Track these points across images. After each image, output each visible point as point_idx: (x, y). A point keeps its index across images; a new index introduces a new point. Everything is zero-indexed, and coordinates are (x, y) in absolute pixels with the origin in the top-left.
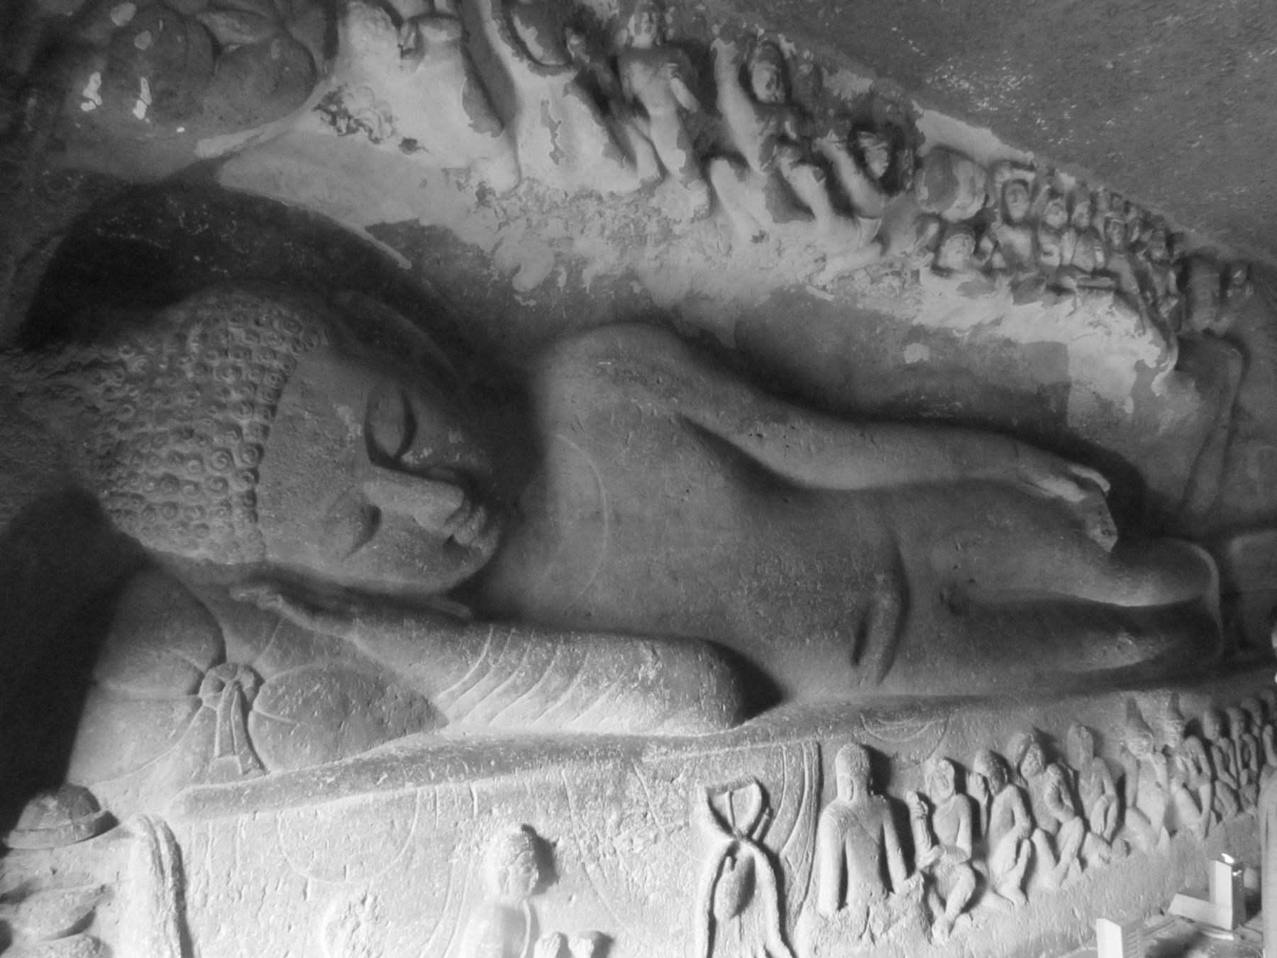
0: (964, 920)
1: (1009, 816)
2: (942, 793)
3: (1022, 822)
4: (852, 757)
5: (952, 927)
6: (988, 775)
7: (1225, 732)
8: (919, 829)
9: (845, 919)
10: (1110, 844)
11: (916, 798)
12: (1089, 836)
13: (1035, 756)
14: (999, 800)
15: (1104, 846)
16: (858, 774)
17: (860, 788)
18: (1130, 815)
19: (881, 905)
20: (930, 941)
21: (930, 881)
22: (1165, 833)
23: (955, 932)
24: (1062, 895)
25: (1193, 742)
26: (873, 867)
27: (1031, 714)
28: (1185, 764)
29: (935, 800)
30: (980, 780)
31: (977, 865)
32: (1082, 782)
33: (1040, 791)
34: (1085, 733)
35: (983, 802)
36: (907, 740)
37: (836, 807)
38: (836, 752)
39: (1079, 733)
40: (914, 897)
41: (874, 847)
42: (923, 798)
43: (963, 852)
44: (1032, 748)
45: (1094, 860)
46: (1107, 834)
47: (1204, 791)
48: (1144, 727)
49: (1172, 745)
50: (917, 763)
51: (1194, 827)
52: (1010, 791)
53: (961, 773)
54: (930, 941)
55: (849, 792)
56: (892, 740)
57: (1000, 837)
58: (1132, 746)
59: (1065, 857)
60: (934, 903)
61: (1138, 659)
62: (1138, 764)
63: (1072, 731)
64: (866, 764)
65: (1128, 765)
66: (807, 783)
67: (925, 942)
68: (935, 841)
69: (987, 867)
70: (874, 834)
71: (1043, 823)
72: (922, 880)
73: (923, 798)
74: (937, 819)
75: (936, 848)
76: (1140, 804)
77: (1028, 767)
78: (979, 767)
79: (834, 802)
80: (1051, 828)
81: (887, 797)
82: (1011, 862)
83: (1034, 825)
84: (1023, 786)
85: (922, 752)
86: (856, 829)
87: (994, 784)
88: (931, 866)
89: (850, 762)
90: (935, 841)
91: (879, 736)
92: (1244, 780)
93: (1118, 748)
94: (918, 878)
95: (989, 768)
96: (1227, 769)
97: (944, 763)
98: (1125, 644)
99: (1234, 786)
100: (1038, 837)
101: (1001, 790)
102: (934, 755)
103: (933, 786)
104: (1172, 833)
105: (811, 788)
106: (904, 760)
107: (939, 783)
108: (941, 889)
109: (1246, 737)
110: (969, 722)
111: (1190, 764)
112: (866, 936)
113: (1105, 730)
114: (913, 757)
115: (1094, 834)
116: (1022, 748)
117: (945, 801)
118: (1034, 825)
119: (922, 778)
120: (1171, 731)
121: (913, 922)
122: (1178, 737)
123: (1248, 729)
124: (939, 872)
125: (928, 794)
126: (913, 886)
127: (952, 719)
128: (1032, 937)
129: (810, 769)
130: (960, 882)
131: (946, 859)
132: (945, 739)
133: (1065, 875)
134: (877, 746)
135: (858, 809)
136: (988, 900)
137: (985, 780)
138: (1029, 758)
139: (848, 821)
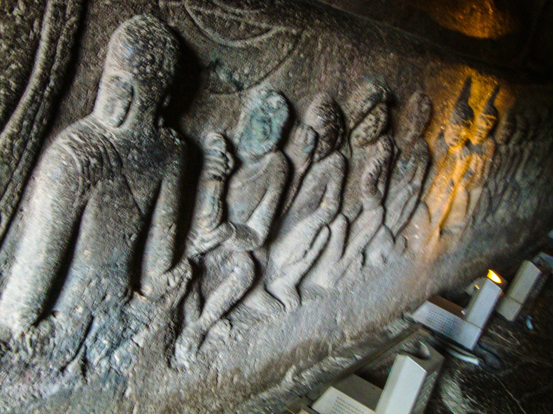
0: (220, 330)
1: (320, 193)
2: (256, 147)
3: (329, 204)
4: (143, 43)
5: (204, 337)
6: (322, 132)
7: (507, 141)
8: (210, 191)
9: (44, 341)
10: (394, 240)
11: (220, 147)
12: (383, 231)
13: (378, 120)
14: (318, 169)
15: (389, 244)
16: (147, 81)
17: (143, 108)
18: (421, 208)
19: (114, 314)
20: (169, 364)
21: (199, 269)
22: (437, 233)
23: (206, 347)
24: (335, 295)
25: (489, 143)
26: (120, 255)
27: (386, 60)
28: (476, 165)
29: (244, 154)
30: (311, 137)
31: (258, 255)
32: (399, 165)
33: (362, 166)
34: (425, 107)
35: (300, 169)
36: (238, 44)
37: (85, 133)
38: (116, 23)
39: (419, 103)
40: (169, 300)
41: (136, 219)
42: (231, 147)
43: (255, 237)
44: (378, 109)
45: (373, 257)
46: (395, 232)
47: (476, 193)
48: (467, 115)
49: (475, 141)
50: (239, 87)
51: (455, 231)
52: (335, 159)
53: (294, 119)
54: (169, 364)
55: (119, 110)
56: (216, 37)
57: (300, 219)
58: (451, 130)
59: (351, 251)
60: (191, 307)
61: (486, 35)
62: (447, 155)
63: (414, 98)
64: (169, 63)
65: (438, 154)
66: (38, 70)
67: (162, 364)
68: (224, 216)
69: (268, 257)
70: (140, 196)
71: (347, 209)
72: (189, 274)
73: (231, 147)
74: (236, 184)
75: (223, 228)
76: (429, 202)
77: (360, 132)
78: (313, 117)
79: (84, 123)
80: (351, 216)
81: (182, 135)
82: (300, 254)
83: (340, 211)
84: (348, 156)
85: (252, 73)
86: (114, 184)
87: (324, 145)
88: (203, 254)
89: (140, 52)
90: (224, 216)
91: (198, 21)
92: (500, 191)
93: (438, 131)
94: (184, 270)
95: (326, 123)
96: (495, 178)
97: (275, 100)
98: (487, 10)
99: (493, 194)
100: (338, 226)
101: (328, 154)
102: (265, 84)
103: (247, 133)
104: (441, 233)
105: (44, 81)
106: (223, 77)
107: (257, 129)
108: (207, 284)
109: (517, 148)
110: (324, 48)
111: (480, 165)
112: (73, 368)
113: (437, 108)
114: (236, 77)
115: (387, 228)
116: (369, 104)
117: (257, 158)
118: (340, 211)
119: (236, 114)
120: (481, 123)
121: (155, 337)
122: (484, 134)
123: (519, 142)
124: (210, 260)
125: (236, 141)
126: (173, 284)
127: (307, 34)
128: (288, 349)
129: (53, 41)
130: (233, 277)
131: (231, 244)
132: (289, 62)
133: (344, 273)
134: (186, 35)
135: (128, 146)
136: (257, 302)
137: (317, 137)
138: (369, 121)
139: (102, 165)
